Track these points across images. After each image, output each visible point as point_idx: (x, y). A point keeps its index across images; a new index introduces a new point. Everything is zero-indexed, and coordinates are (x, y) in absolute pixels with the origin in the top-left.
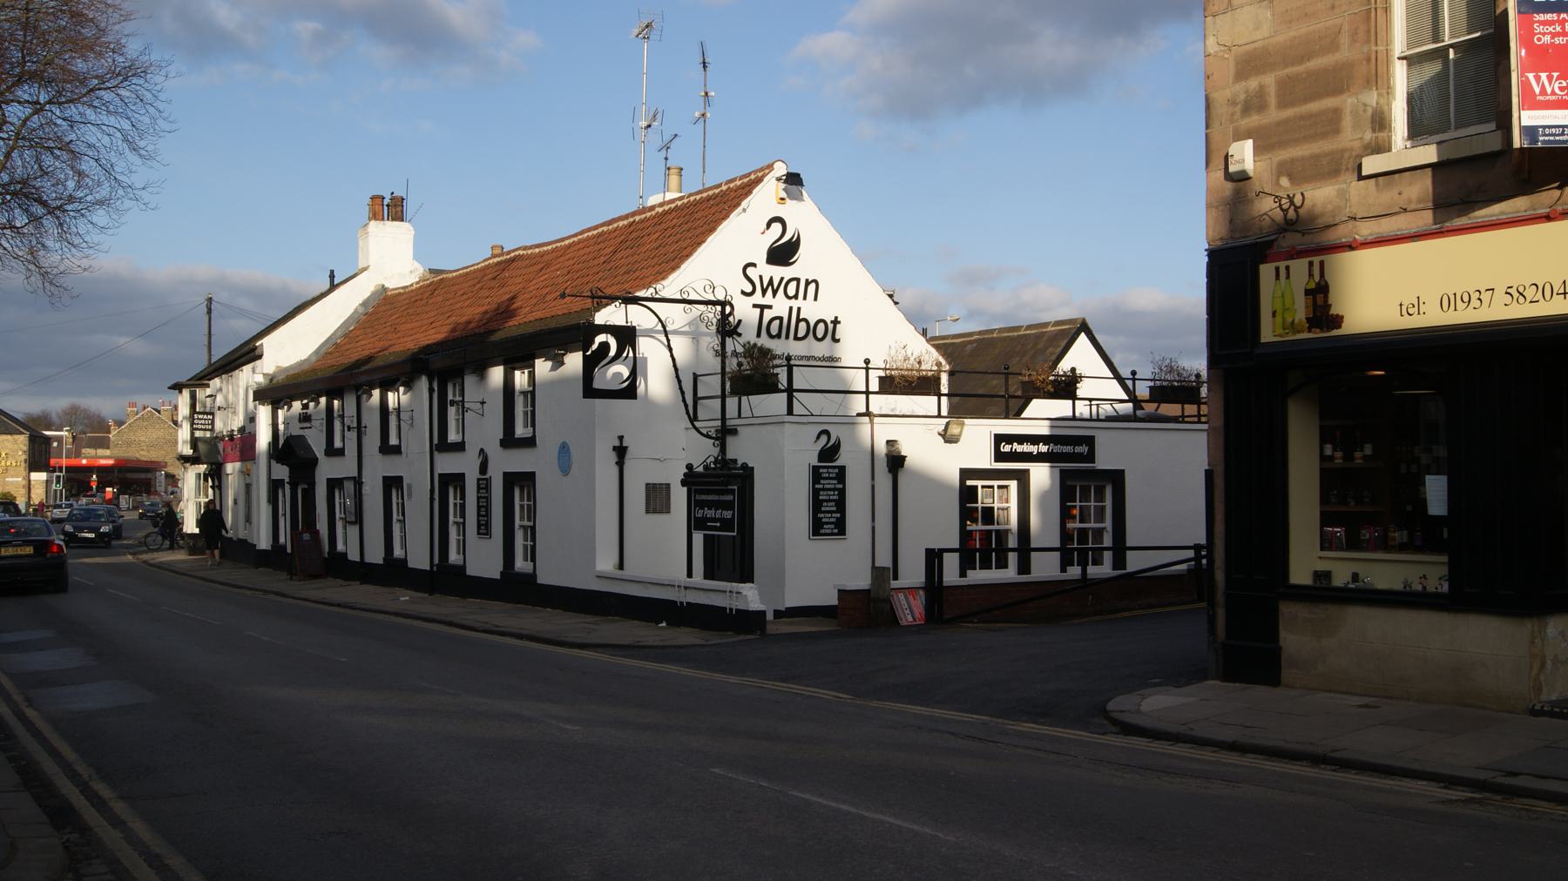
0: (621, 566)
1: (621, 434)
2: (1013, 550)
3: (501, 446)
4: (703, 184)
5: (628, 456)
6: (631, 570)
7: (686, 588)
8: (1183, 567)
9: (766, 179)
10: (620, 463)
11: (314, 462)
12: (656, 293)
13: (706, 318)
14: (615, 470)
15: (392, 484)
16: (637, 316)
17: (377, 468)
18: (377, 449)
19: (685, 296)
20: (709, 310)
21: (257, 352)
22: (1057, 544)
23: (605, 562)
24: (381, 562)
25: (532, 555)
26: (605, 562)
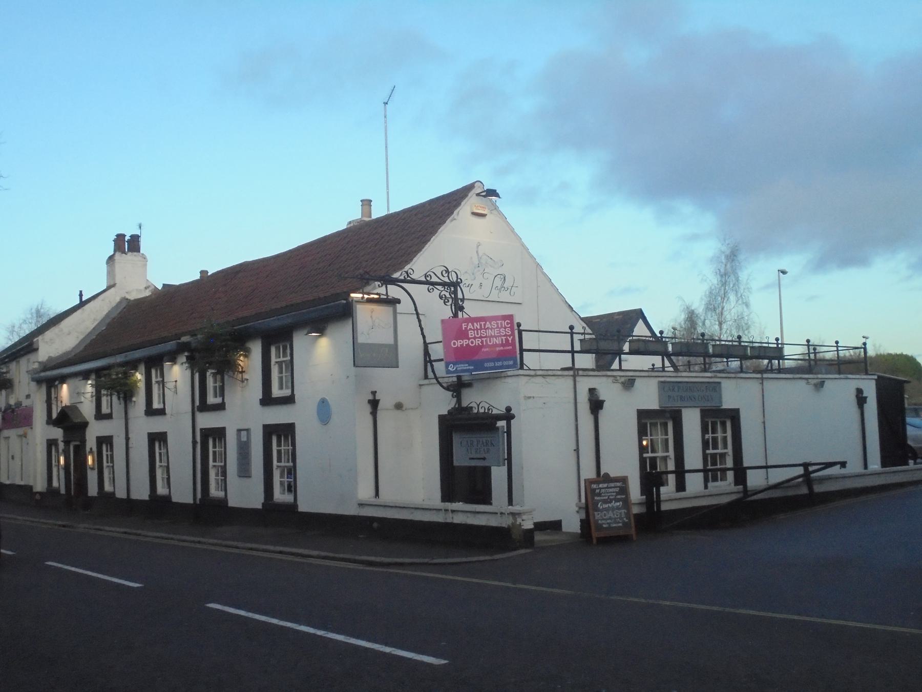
2: (671, 472)
4: (388, 210)
6: (387, 496)
7: (453, 511)
8: (800, 480)
9: (470, 195)
10: (374, 413)
11: (85, 425)
12: (408, 276)
13: (444, 296)
14: (369, 419)
15: (157, 439)
16: (394, 291)
17: (142, 426)
18: (143, 413)
19: (428, 279)
20: (446, 290)
21: (35, 346)
22: (701, 467)
23: (365, 492)
24: (147, 498)
25: (291, 488)
26: (365, 492)
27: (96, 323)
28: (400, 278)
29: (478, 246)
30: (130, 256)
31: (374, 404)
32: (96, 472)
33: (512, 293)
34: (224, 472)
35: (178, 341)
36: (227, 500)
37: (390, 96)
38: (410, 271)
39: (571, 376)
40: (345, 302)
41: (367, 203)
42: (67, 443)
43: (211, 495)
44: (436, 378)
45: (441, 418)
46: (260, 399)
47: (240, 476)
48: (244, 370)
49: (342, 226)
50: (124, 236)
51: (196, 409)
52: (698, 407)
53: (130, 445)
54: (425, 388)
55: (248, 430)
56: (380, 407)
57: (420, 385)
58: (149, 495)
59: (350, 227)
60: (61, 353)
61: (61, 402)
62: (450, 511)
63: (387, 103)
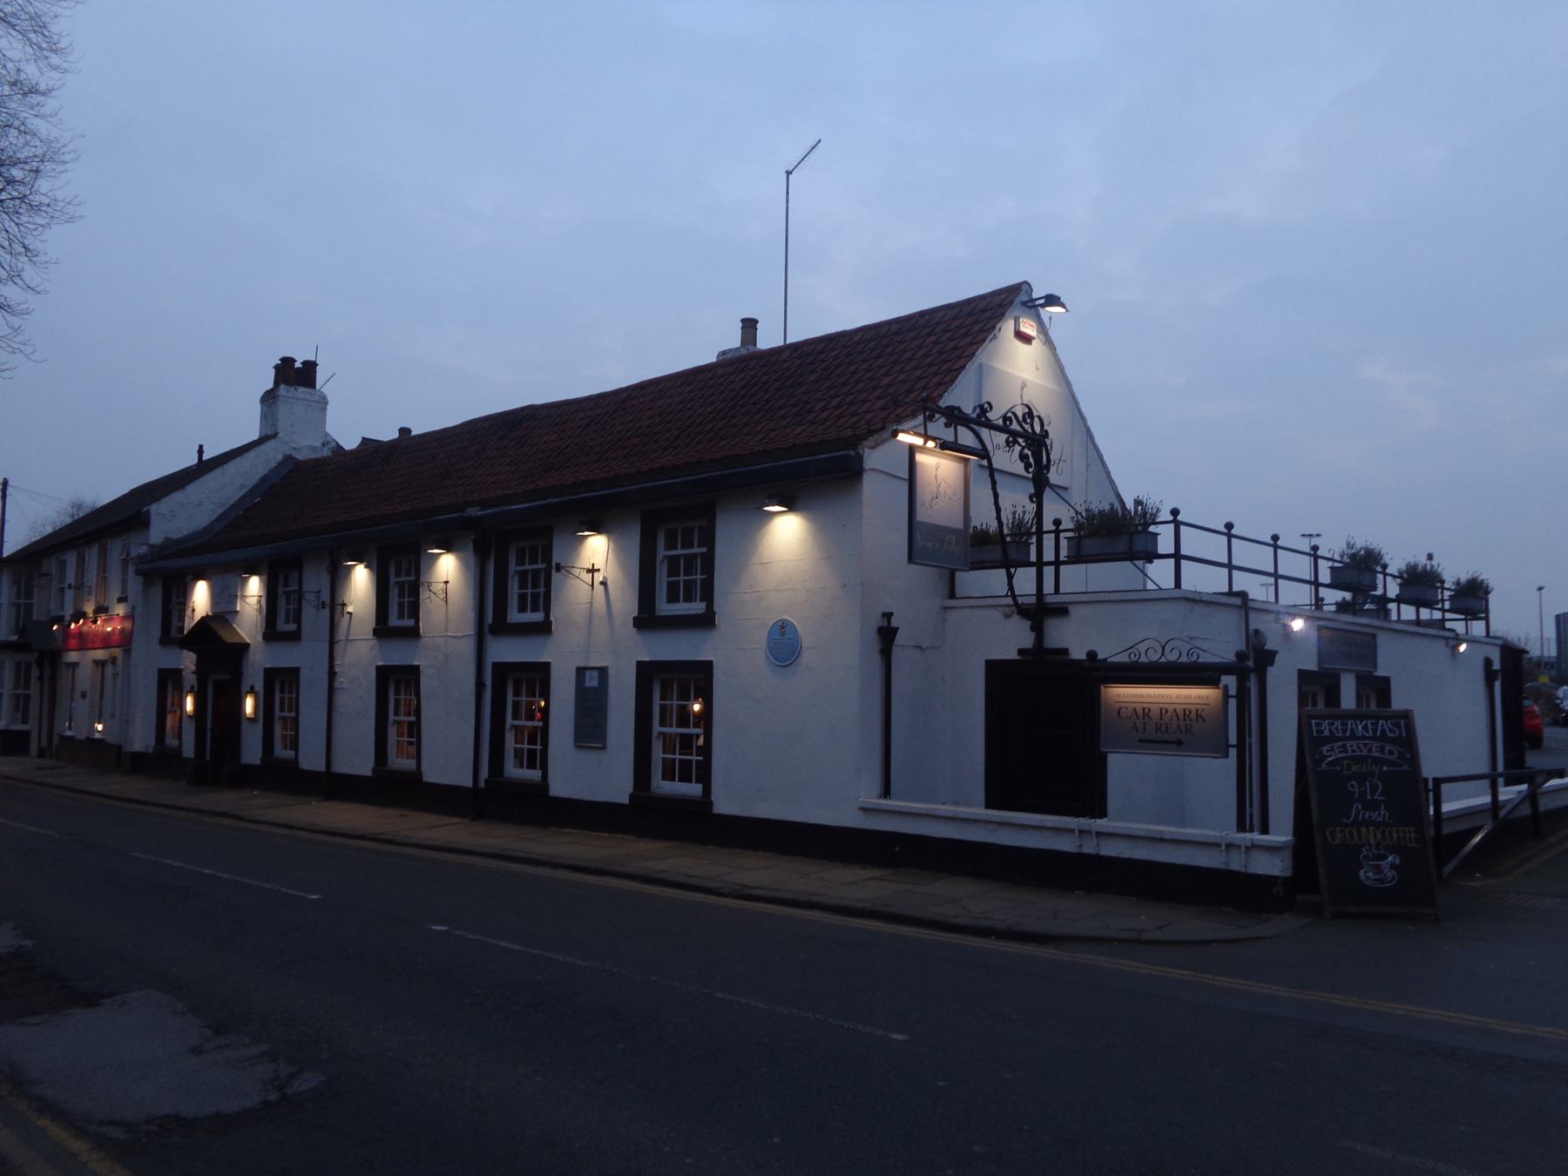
0: (886, 792)
1: (888, 610)
3: (635, 626)
4: (785, 339)
5: (899, 639)
7: (1099, 834)
10: (886, 651)
27: (244, 491)
28: (972, 416)
29: (1022, 388)
30: (302, 391)
31: (887, 634)
32: (260, 725)
33: (1060, 471)
34: (541, 735)
35: (462, 514)
36: (421, 774)
37: (803, 159)
38: (986, 406)
39: (1236, 606)
40: (853, 453)
41: (749, 325)
42: (201, 673)
43: (506, 775)
44: (1014, 596)
45: (993, 667)
46: (634, 618)
47: (578, 747)
48: (596, 567)
49: (710, 358)
50: (293, 361)
51: (486, 629)
52: (1351, 671)
53: (337, 685)
54: (952, 616)
55: (603, 671)
56: (895, 643)
57: (945, 608)
58: (630, 795)
59: (721, 361)
60: (185, 533)
61: (193, 610)
62: (1094, 834)
63: (791, 173)
